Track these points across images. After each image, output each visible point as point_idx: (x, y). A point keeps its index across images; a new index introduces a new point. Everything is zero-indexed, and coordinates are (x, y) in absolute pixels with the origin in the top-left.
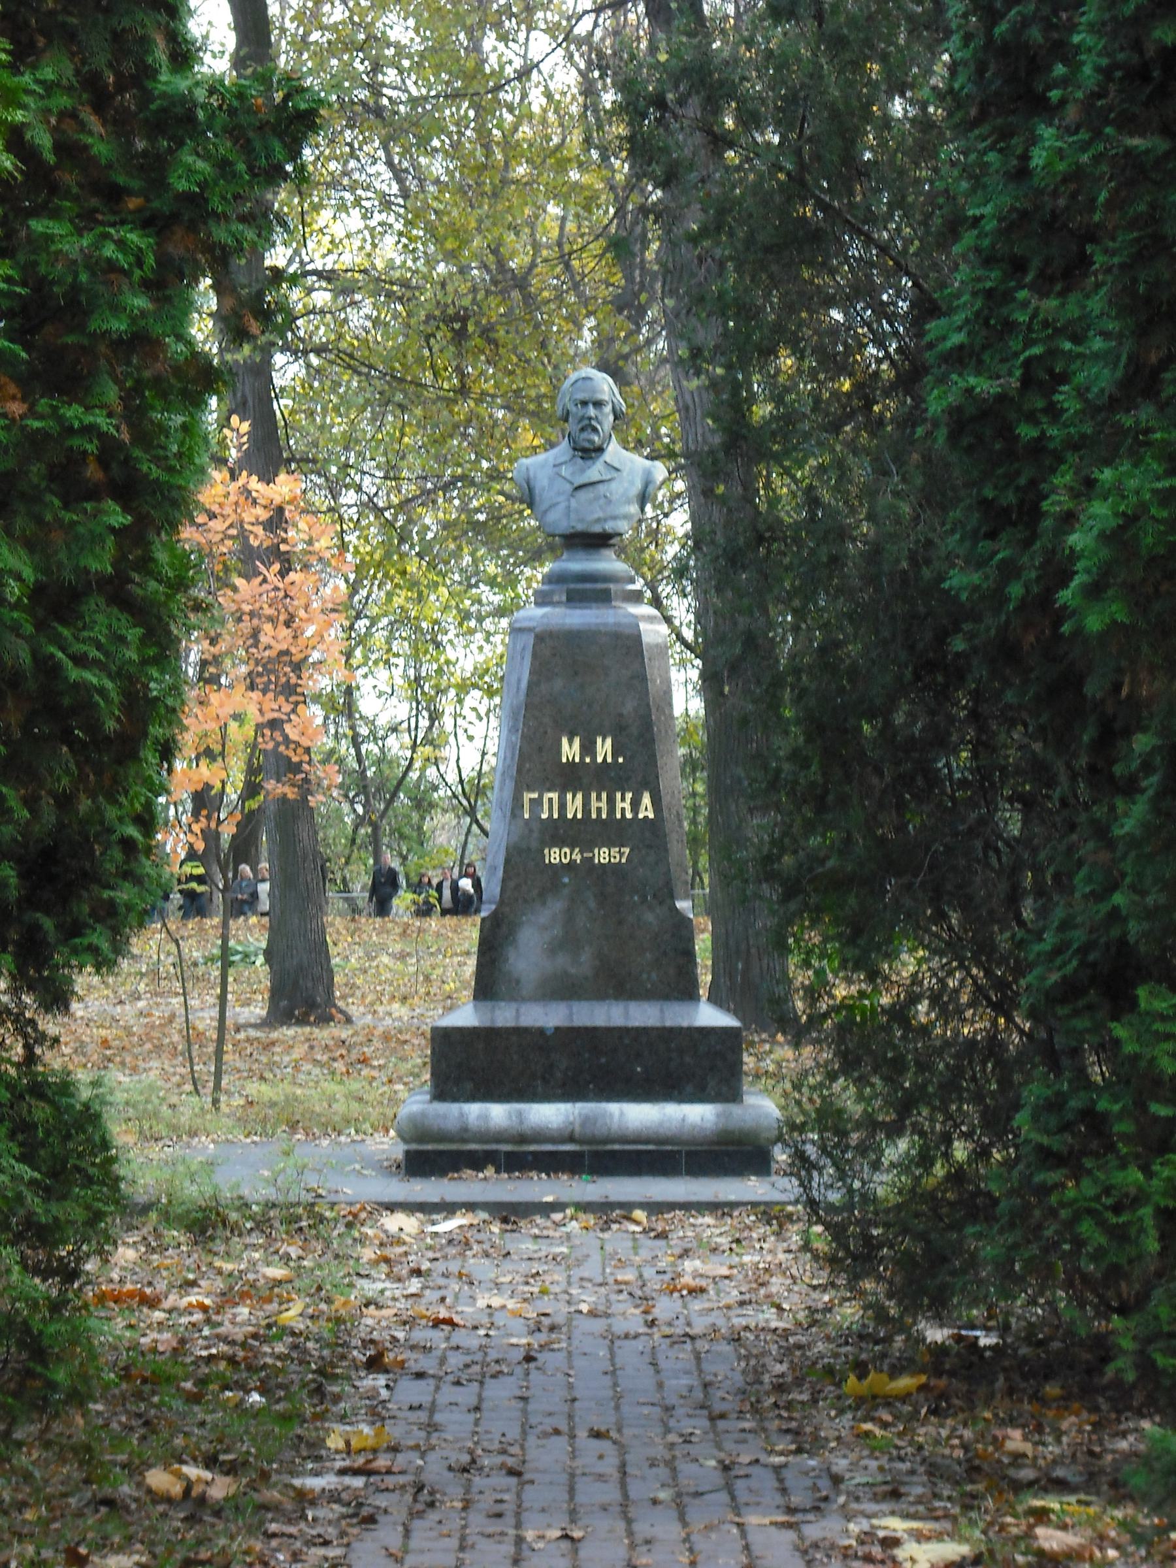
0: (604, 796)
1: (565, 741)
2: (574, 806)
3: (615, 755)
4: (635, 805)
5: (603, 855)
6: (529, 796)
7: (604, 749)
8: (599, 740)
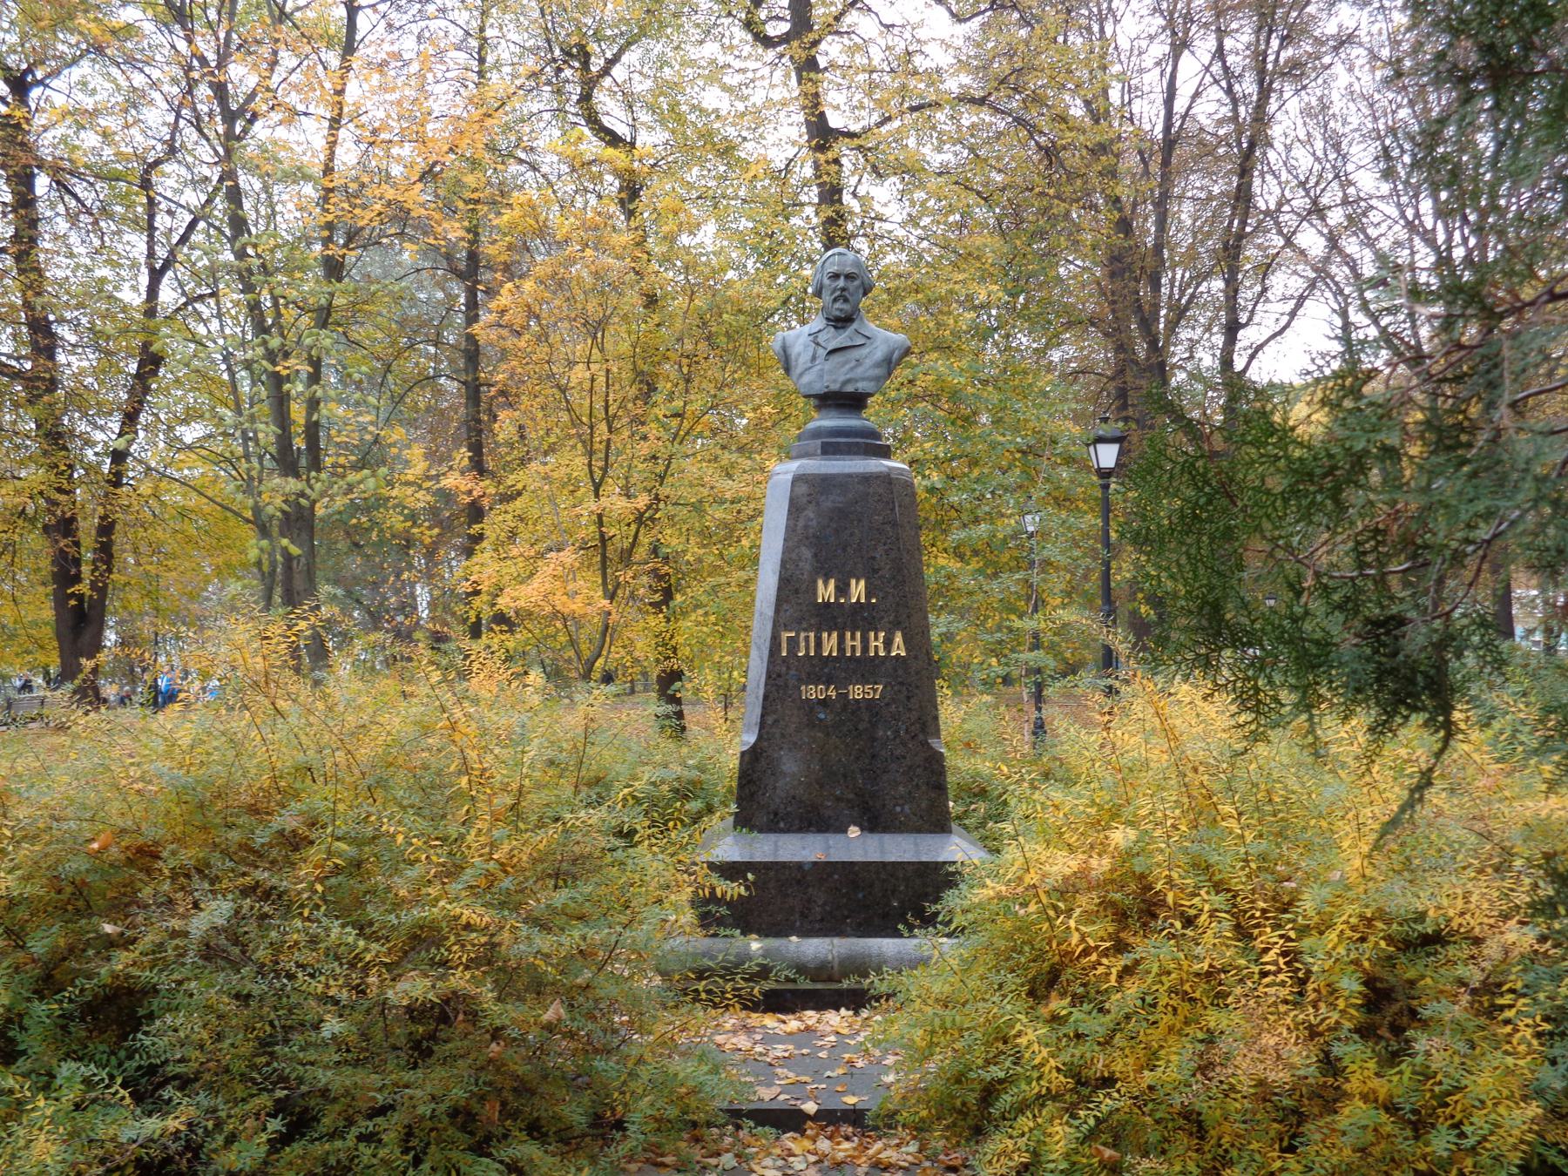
0: (858, 634)
1: (820, 583)
2: (830, 644)
3: (868, 595)
4: (888, 643)
5: (857, 692)
6: (785, 635)
7: (858, 590)
8: (853, 582)
